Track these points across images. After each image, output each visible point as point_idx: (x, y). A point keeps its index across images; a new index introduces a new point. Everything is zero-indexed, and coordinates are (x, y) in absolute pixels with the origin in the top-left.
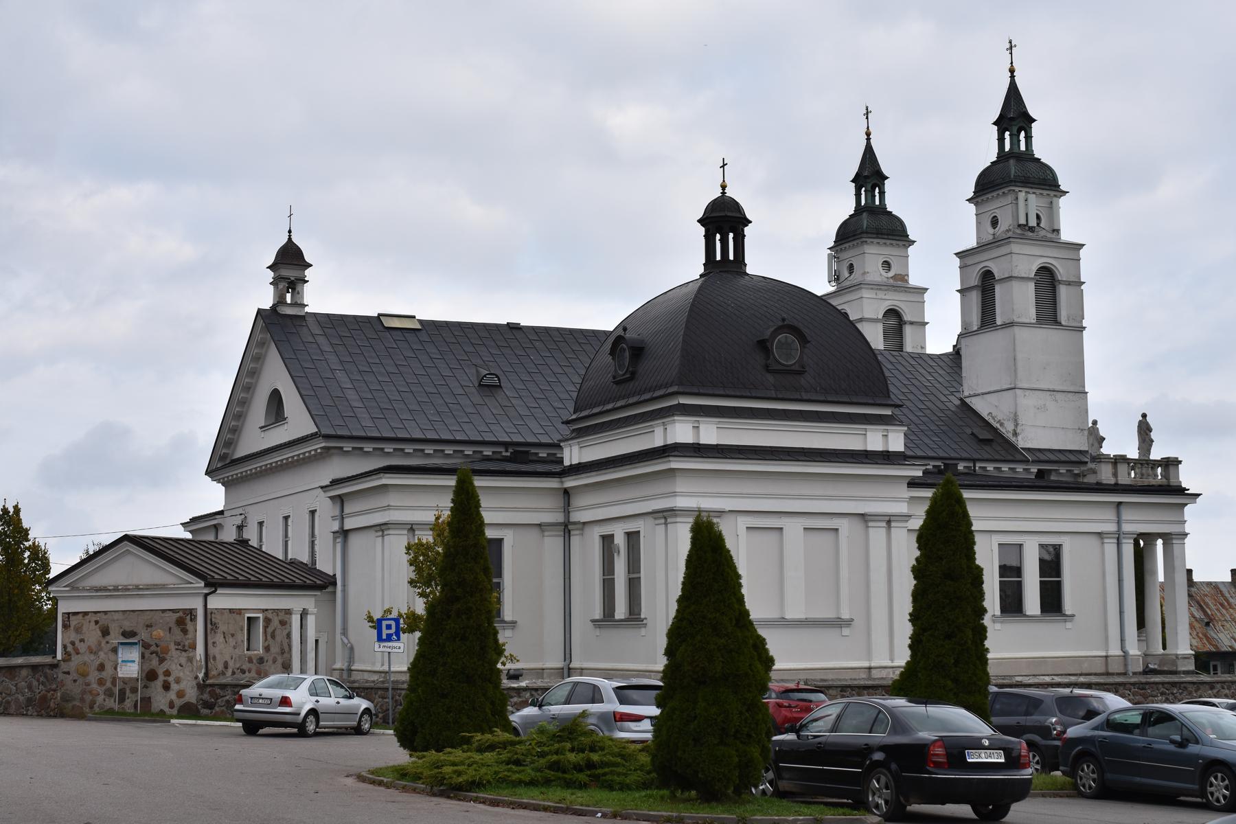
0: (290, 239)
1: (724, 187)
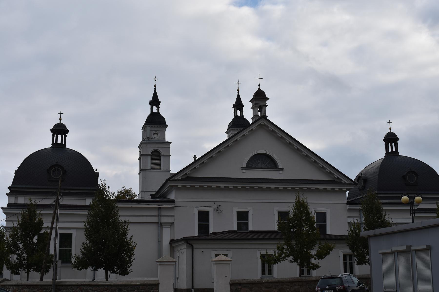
0: (259, 88)
1: (390, 129)
